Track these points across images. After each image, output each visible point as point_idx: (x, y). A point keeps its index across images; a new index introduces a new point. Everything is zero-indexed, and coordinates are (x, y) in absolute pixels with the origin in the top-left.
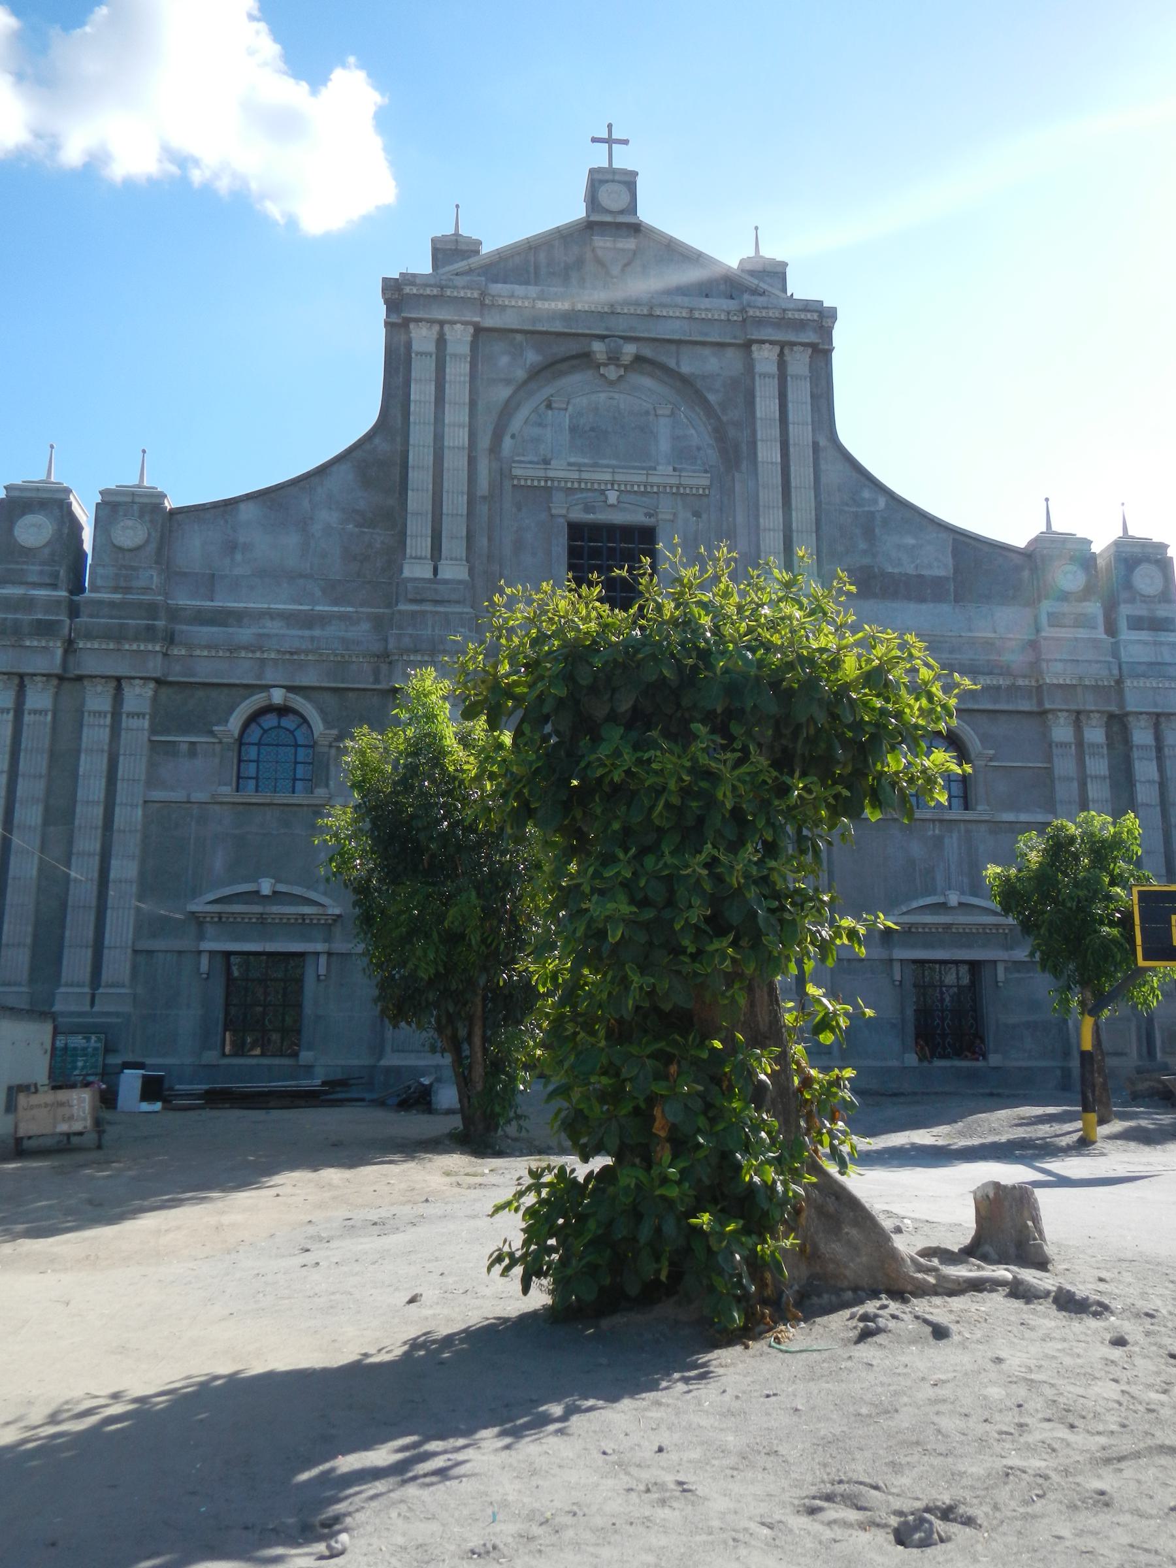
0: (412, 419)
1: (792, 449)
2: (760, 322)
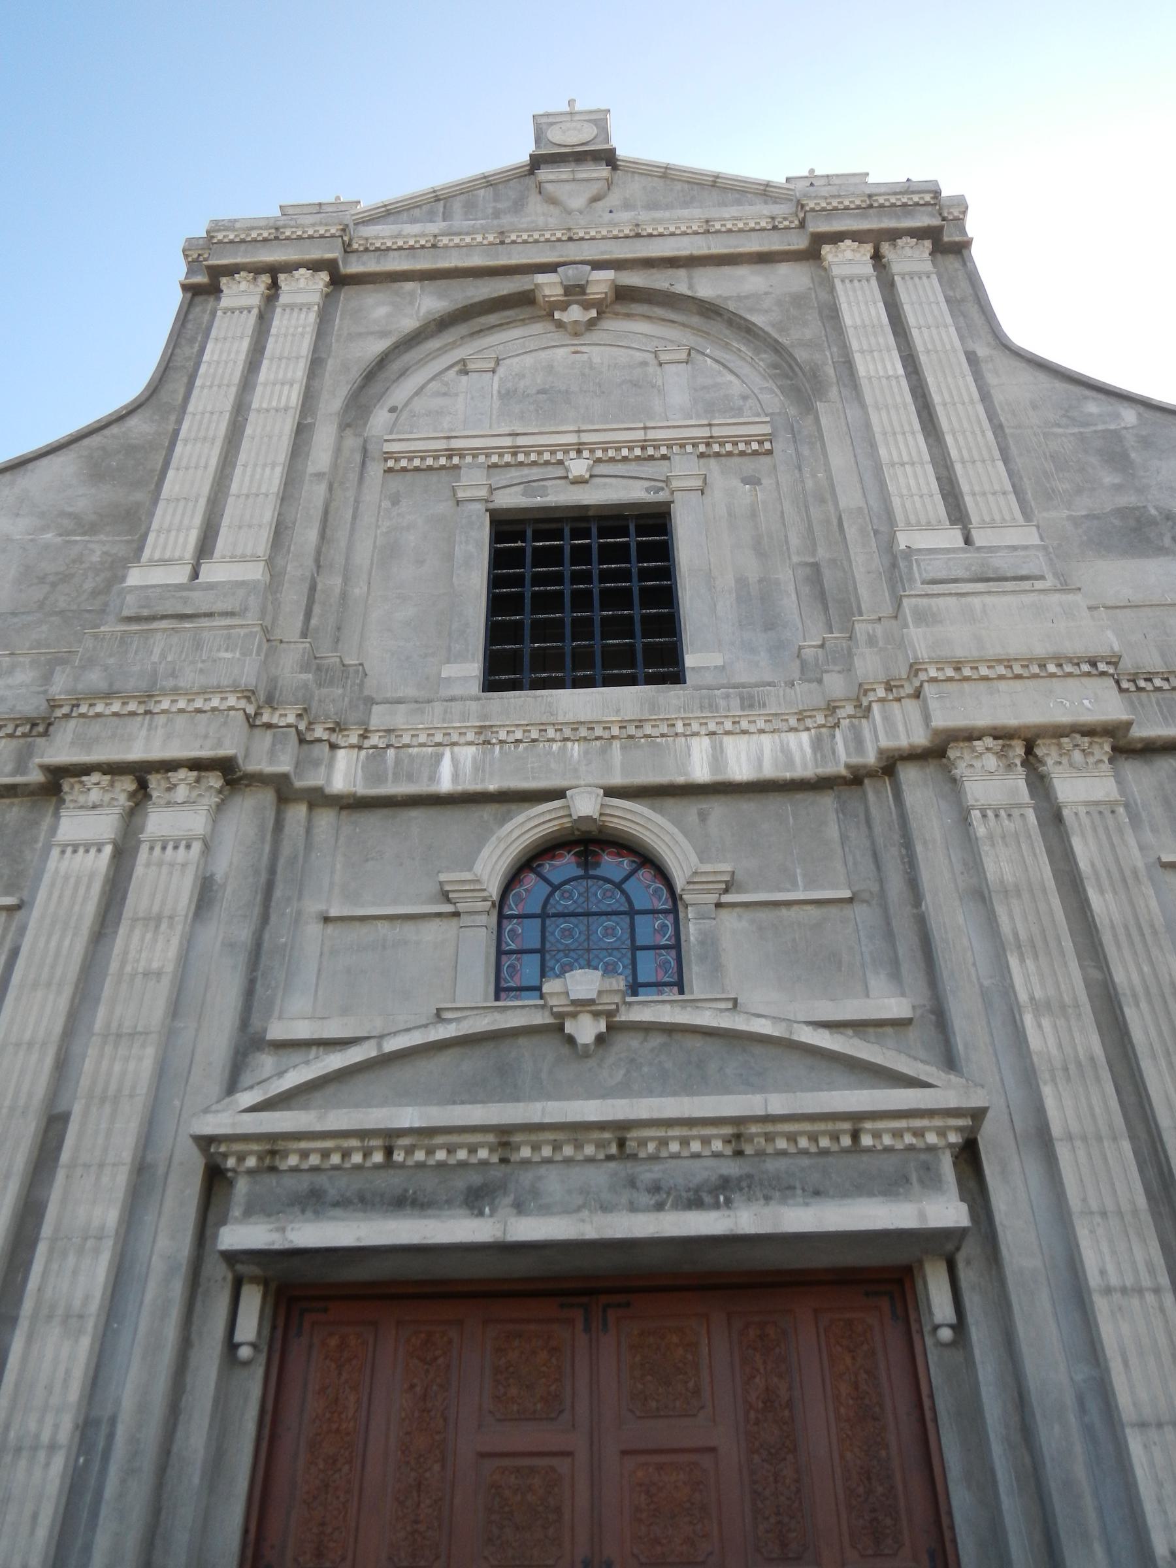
0: (198, 382)
1: (923, 358)
2: (832, 213)
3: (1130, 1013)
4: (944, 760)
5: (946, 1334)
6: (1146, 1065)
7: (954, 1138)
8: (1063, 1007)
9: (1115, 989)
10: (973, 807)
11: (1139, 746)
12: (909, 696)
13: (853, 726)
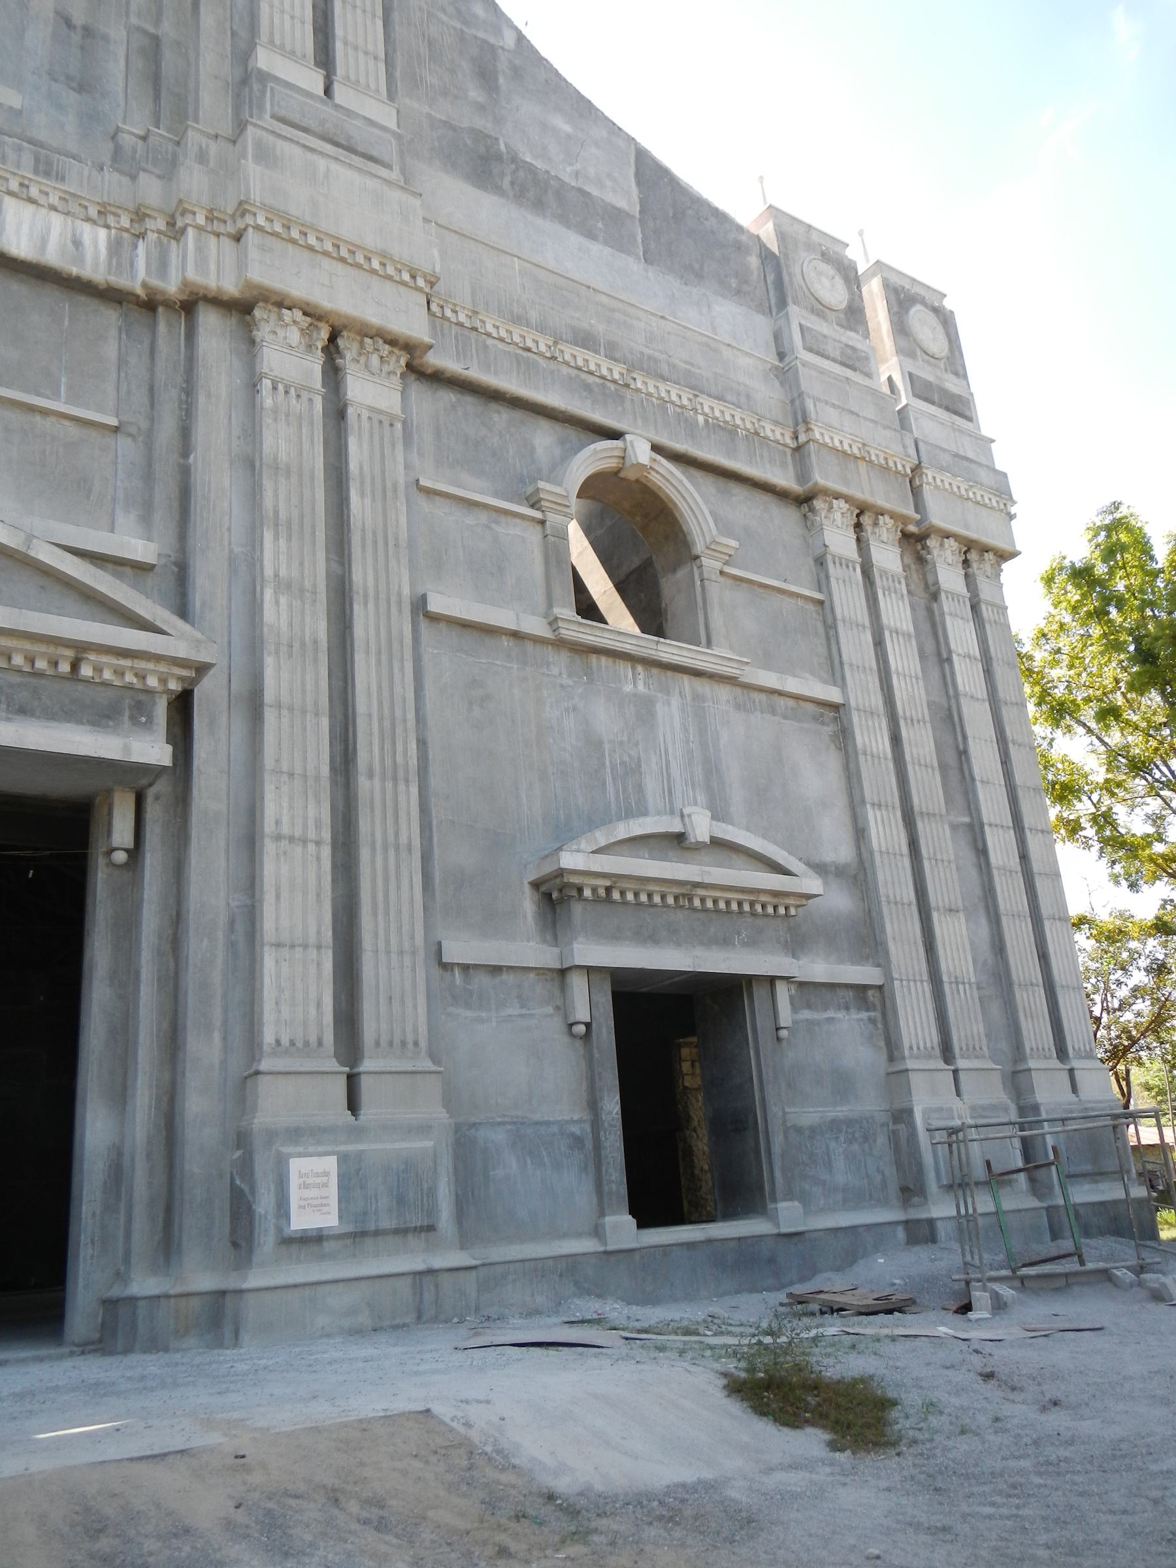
3: (357, 609)
4: (248, 317)
5: (120, 857)
6: (359, 659)
7: (174, 685)
8: (302, 590)
9: (351, 589)
10: (266, 376)
11: (429, 371)
12: (229, 235)
13: (160, 242)
